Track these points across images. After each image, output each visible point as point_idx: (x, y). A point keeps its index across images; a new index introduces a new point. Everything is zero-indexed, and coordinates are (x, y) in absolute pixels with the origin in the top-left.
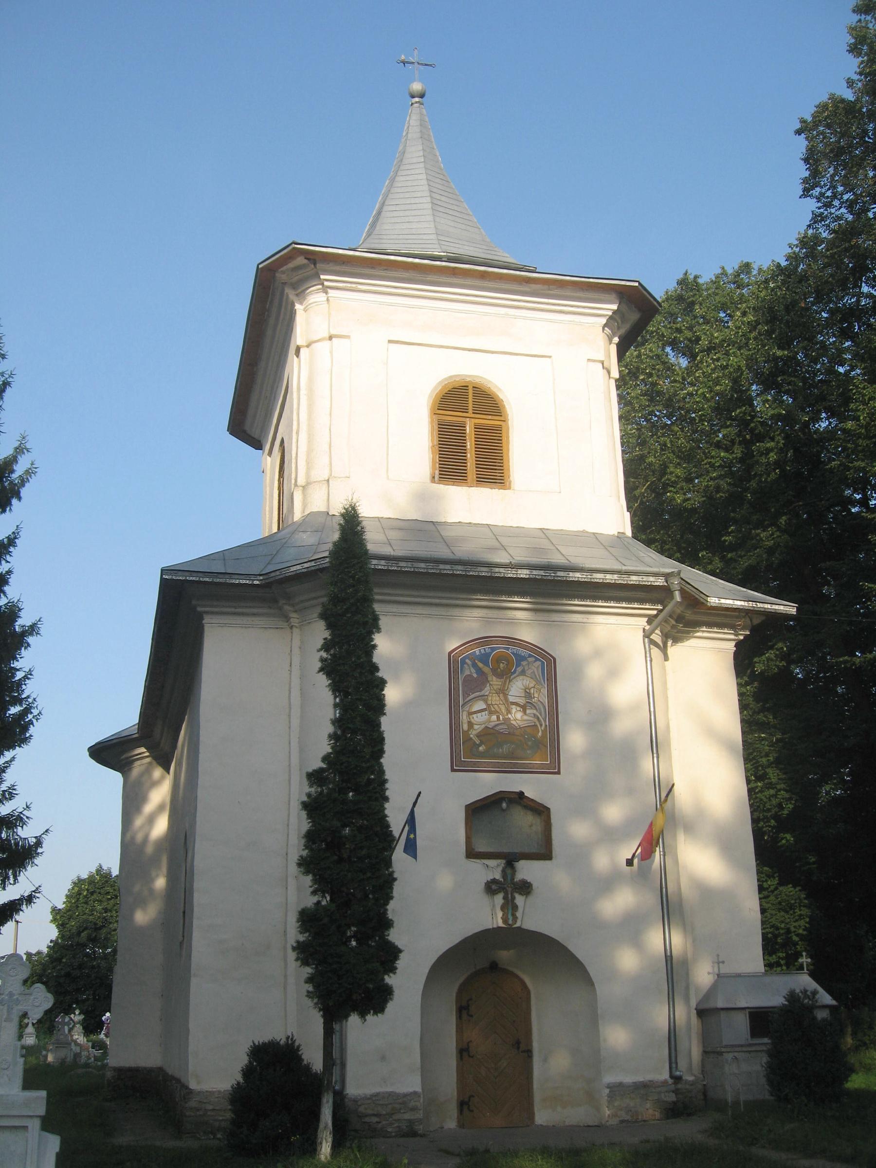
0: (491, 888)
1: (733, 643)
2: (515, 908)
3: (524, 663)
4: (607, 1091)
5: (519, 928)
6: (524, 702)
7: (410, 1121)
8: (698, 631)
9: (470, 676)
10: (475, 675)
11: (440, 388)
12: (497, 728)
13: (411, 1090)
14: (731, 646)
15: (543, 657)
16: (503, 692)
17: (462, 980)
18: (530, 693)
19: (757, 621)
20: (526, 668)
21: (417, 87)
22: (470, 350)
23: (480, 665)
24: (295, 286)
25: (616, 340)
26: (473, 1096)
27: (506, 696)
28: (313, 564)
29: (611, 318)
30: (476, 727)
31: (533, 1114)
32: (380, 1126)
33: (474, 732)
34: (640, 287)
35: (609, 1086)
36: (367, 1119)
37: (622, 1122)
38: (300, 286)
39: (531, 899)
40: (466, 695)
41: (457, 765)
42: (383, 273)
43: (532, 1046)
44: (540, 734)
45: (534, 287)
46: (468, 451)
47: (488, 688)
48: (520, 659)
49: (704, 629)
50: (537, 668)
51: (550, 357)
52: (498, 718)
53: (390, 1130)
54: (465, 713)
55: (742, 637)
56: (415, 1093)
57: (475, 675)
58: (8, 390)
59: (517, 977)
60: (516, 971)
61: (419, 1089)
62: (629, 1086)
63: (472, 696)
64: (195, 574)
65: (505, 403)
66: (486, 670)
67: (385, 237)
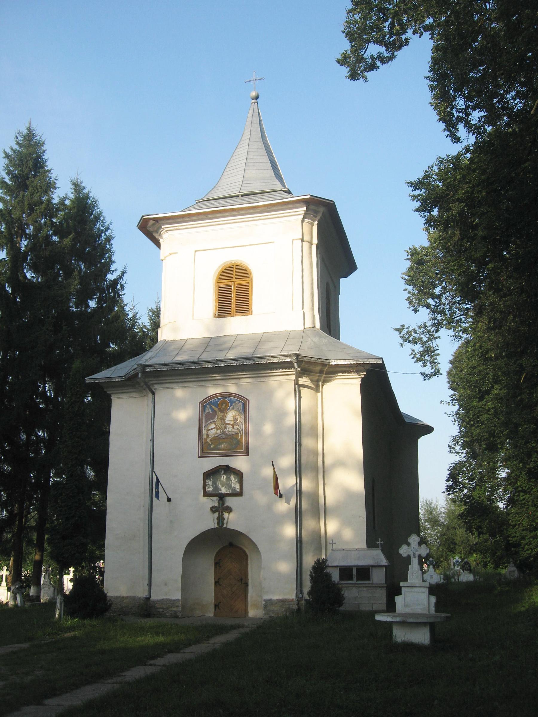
0: (213, 510)
1: (360, 379)
3: (234, 404)
4: (264, 603)
5: (226, 528)
6: (233, 423)
8: (336, 376)
9: (209, 413)
10: (211, 412)
11: (220, 269)
12: (219, 436)
13: (177, 598)
14: (359, 381)
16: (223, 419)
17: (217, 551)
18: (235, 418)
19: (368, 368)
21: (253, 94)
23: (213, 407)
25: (316, 223)
26: (220, 603)
27: (224, 420)
29: (305, 214)
30: (210, 436)
31: (248, 612)
32: (163, 613)
33: (209, 439)
34: (312, 197)
35: (265, 601)
36: (158, 610)
40: (206, 421)
41: (201, 454)
43: (248, 581)
45: (261, 209)
46: (232, 299)
49: (340, 374)
51: (274, 242)
52: (220, 431)
53: (167, 615)
54: (205, 430)
55: (363, 376)
56: (178, 600)
57: (211, 412)
58: (125, 274)
61: (180, 598)
62: (275, 601)
63: (209, 422)
64: (92, 380)
65: (252, 271)
66: (216, 409)
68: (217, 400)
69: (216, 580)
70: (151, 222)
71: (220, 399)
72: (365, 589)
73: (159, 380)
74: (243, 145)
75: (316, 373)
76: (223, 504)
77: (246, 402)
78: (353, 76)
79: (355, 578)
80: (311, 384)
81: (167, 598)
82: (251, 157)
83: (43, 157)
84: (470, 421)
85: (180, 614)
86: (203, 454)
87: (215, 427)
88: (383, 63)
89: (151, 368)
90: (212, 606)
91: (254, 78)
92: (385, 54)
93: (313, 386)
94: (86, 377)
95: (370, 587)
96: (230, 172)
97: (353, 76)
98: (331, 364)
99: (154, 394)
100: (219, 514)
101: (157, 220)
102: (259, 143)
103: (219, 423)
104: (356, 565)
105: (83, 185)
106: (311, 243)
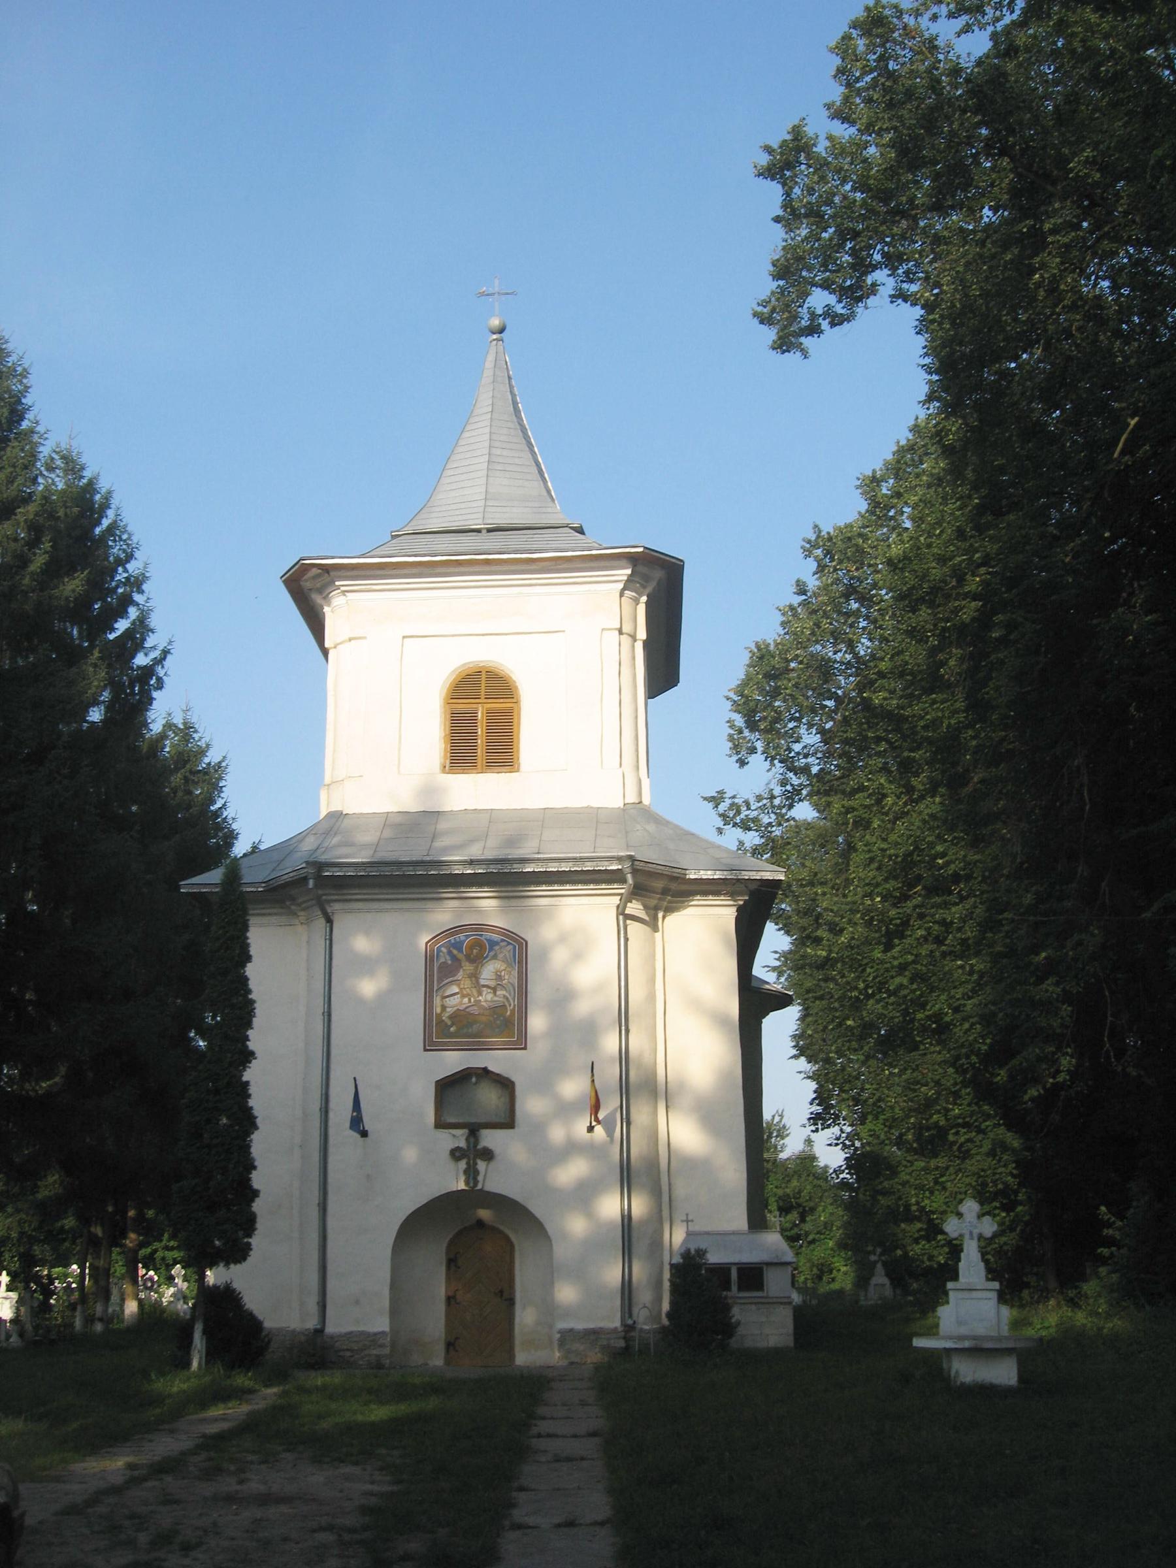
1: (734, 909)
2: (477, 1172)
3: (497, 948)
4: (558, 1336)
5: (481, 1190)
7: (377, 1356)
10: (450, 962)
13: (380, 1330)
15: (516, 940)
16: (475, 976)
19: (753, 887)
20: (498, 952)
21: (495, 322)
22: (483, 635)
23: (455, 952)
24: (320, 591)
25: (644, 599)
27: (477, 979)
28: (295, 873)
29: (627, 581)
30: (448, 1010)
32: (352, 1359)
33: (447, 1015)
34: (647, 551)
35: (559, 1332)
36: (341, 1354)
37: (572, 1363)
39: (493, 1164)
40: (440, 980)
41: (430, 1045)
44: (509, 1013)
47: (461, 972)
48: (493, 944)
49: (698, 897)
52: (470, 1000)
53: (361, 1363)
54: (438, 999)
55: (741, 903)
56: (383, 1333)
57: (450, 962)
58: (169, 657)
59: (500, 1232)
60: (502, 1228)
61: (387, 1329)
66: (460, 956)
67: (437, 509)
69: (450, 1294)
70: (315, 571)
71: (467, 936)
72: (753, 1307)
74: (480, 424)
75: (657, 893)
76: (477, 1142)
77: (520, 945)
78: (784, 344)
79: (734, 1288)
80: (642, 914)
81: (361, 1328)
82: (498, 452)
83: (24, 401)
84: (867, 987)
85: (388, 1361)
86: (432, 1043)
87: (457, 990)
88: (833, 324)
89: (335, 869)
90: (440, 1348)
91: (497, 289)
92: (839, 309)
93: (647, 918)
94: (183, 880)
95: (764, 1303)
96: (453, 479)
97: (784, 344)
98: (687, 877)
99: (329, 921)
100: (468, 1163)
101: (326, 569)
102: (510, 425)
103: (467, 983)
105: (83, 460)
106: (634, 638)
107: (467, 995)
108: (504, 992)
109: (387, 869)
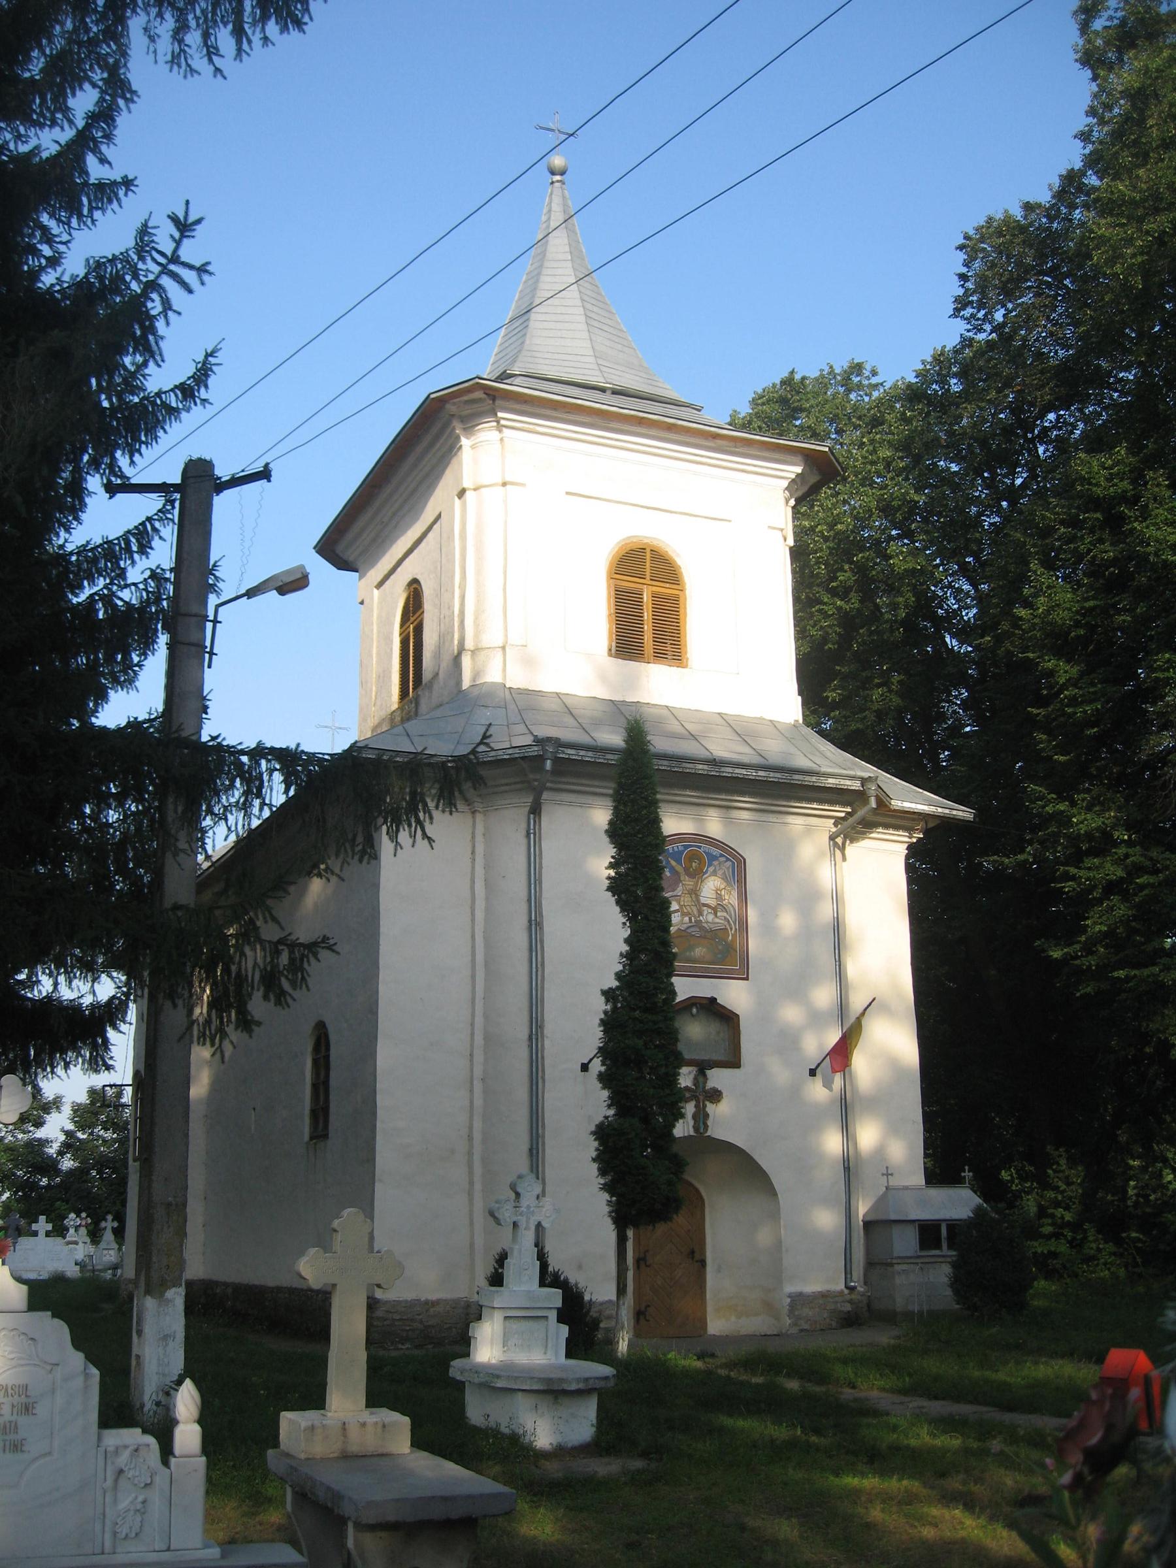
3: (715, 863)
8: (872, 833)
12: (689, 931)
13: (606, 1299)
14: (902, 850)
15: (734, 857)
26: (649, 1306)
27: (697, 896)
29: (793, 481)
37: (802, 1331)
38: (470, 422)
42: (564, 416)
45: (719, 442)
46: (645, 622)
47: (680, 888)
48: (712, 858)
49: (880, 830)
50: (728, 868)
52: (690, 919)
55: (914, 840)
59: (691, 1185)
66: (679, 868)
68: (681, 848)
71: (686, 847)
73: (560, 783)
77: (739, 862)
79: (944, 1245)
104: (948, 1218)
107: (687, 914)
108: (725, 914)
109: (665, 763)
